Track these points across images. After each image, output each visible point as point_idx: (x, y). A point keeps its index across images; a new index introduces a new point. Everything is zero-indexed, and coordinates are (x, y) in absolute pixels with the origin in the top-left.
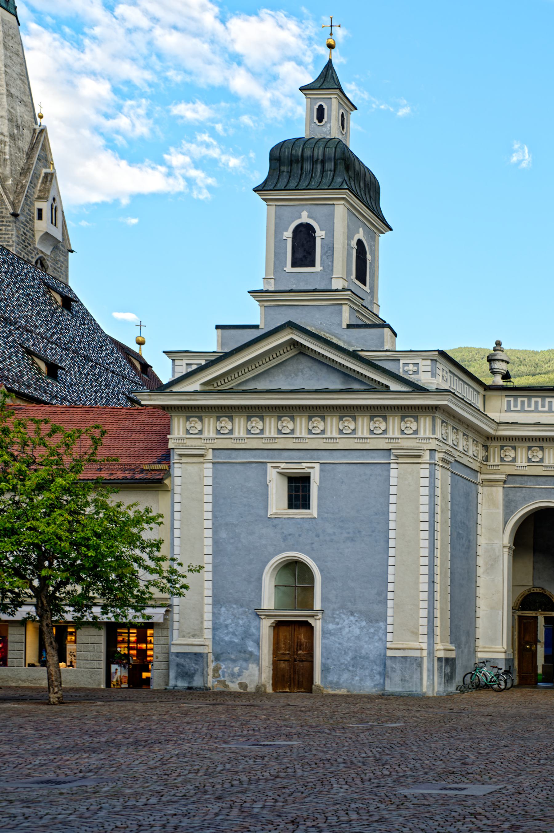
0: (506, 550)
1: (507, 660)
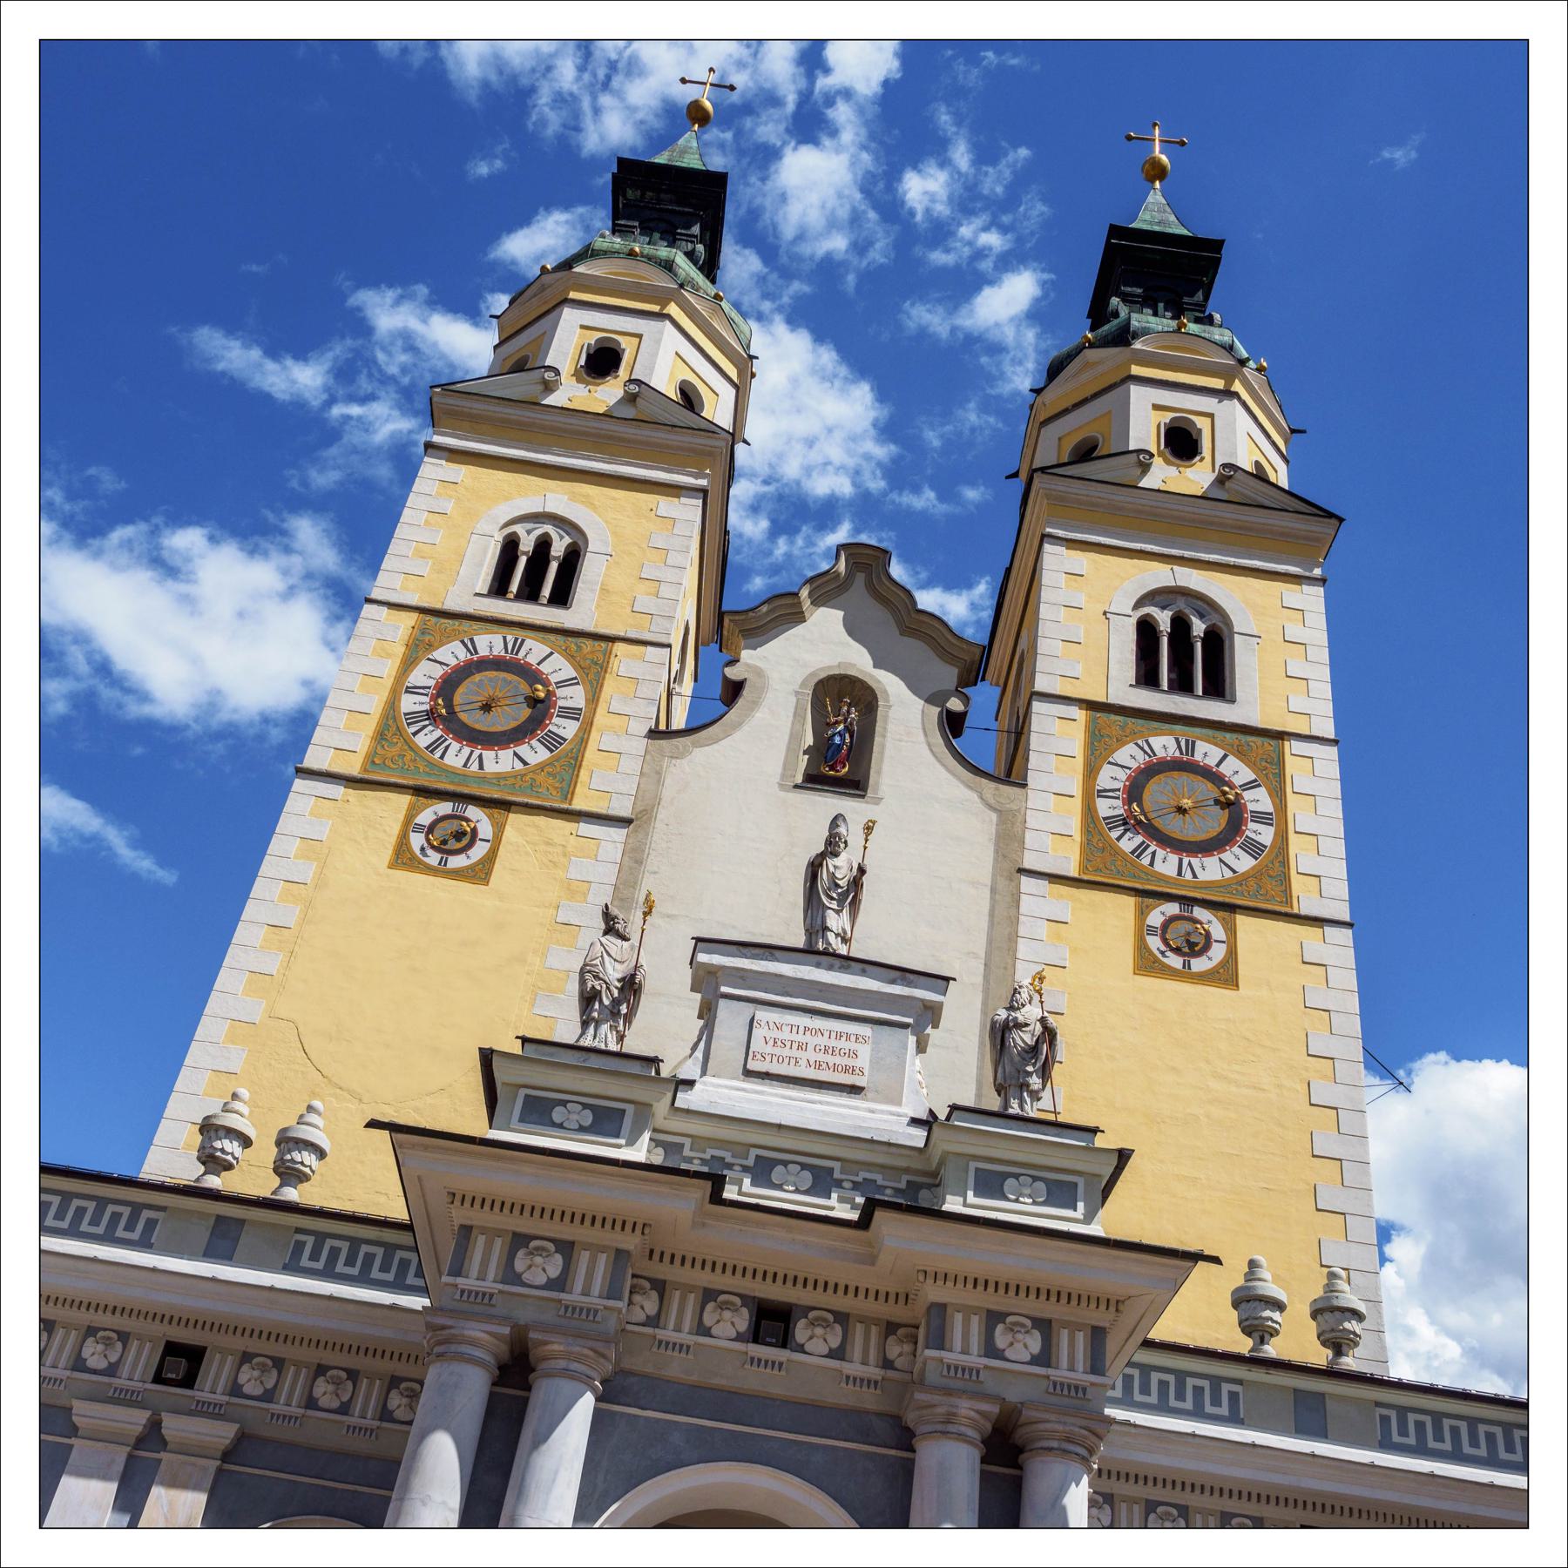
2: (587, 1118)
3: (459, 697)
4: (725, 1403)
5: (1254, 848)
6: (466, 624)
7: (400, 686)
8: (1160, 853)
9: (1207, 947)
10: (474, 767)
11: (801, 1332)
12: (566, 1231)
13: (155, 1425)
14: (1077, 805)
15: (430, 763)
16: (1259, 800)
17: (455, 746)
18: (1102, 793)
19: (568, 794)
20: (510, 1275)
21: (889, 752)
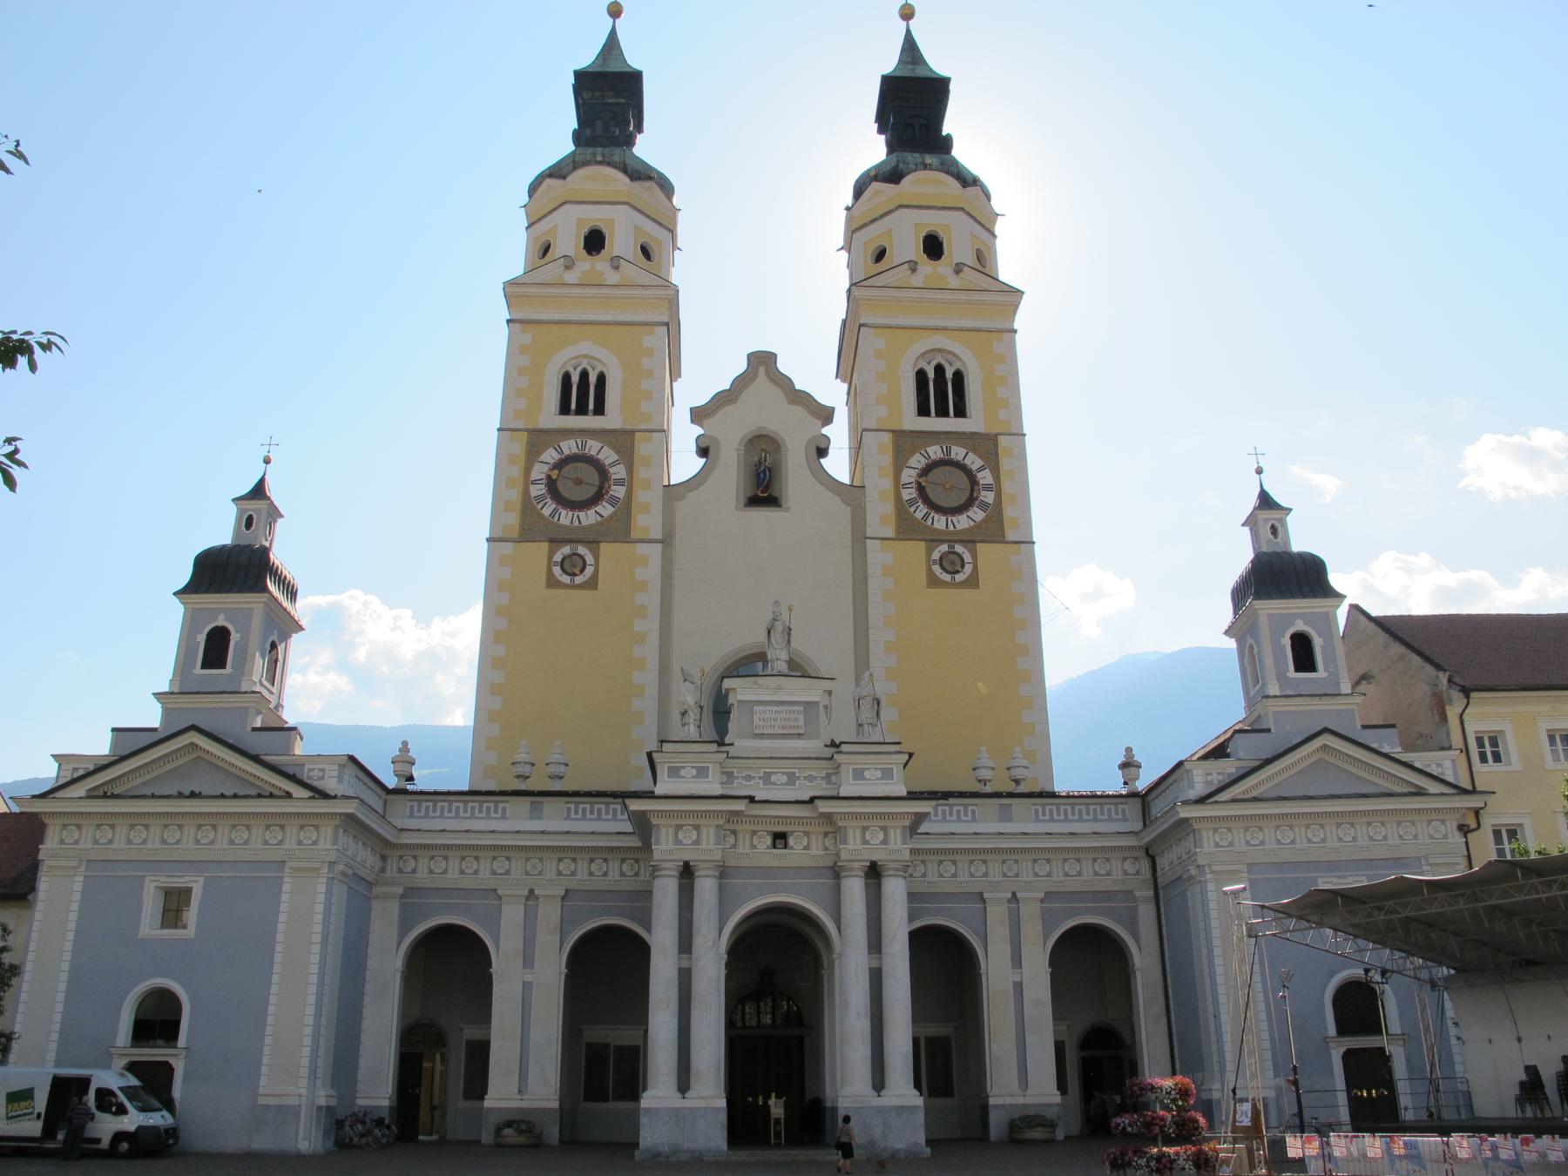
0: (399, 975)
1: (391, 1108)
2: (694, 772)
4: (766, 872)
5: (984, 506)
7: (528, 482)
11: (791, 841)
12: (696, 822)
13: (531, 891)
17: (564, 512)
18: (905, 486)
19: (628, 531)
20: (678, 842)
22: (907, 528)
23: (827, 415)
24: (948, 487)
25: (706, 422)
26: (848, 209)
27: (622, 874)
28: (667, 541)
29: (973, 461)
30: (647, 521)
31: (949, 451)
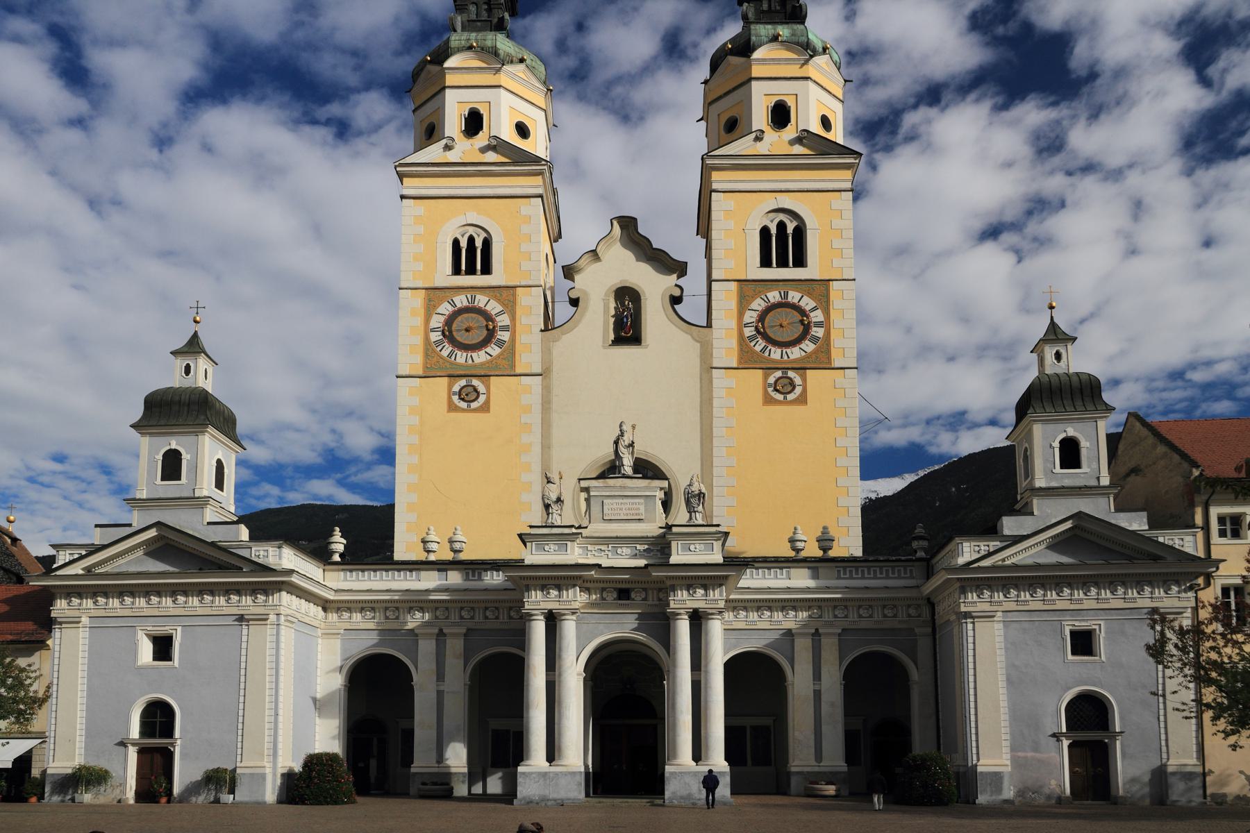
3: (454, 326)
5: (815, 340)
6: (448, 293)
7: (428, 330)
8: (773, 349)
9: (794, 388)
10: (470, 361)
13: (441, 630)
14: (735, 333)
15: (451, 363)
16: (817, 316)
17: (459, 353)
18: (746, 325)
19: (513, 366)
21: (648, 317)
22: (748, 360)
23: (680, 269)
24: (786, 324)
25: (577, 277)
26: (706, 82)
27: (510, 617)
28: (545, 374)
29: (807, 303)
30: (528, 358)
31: (786, 294)
